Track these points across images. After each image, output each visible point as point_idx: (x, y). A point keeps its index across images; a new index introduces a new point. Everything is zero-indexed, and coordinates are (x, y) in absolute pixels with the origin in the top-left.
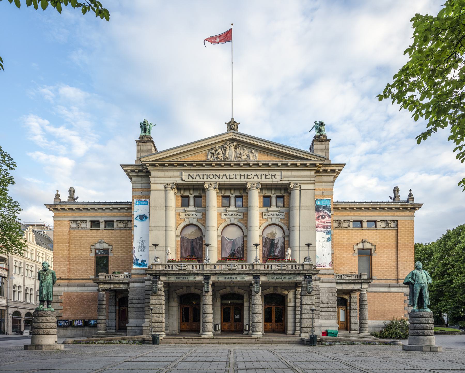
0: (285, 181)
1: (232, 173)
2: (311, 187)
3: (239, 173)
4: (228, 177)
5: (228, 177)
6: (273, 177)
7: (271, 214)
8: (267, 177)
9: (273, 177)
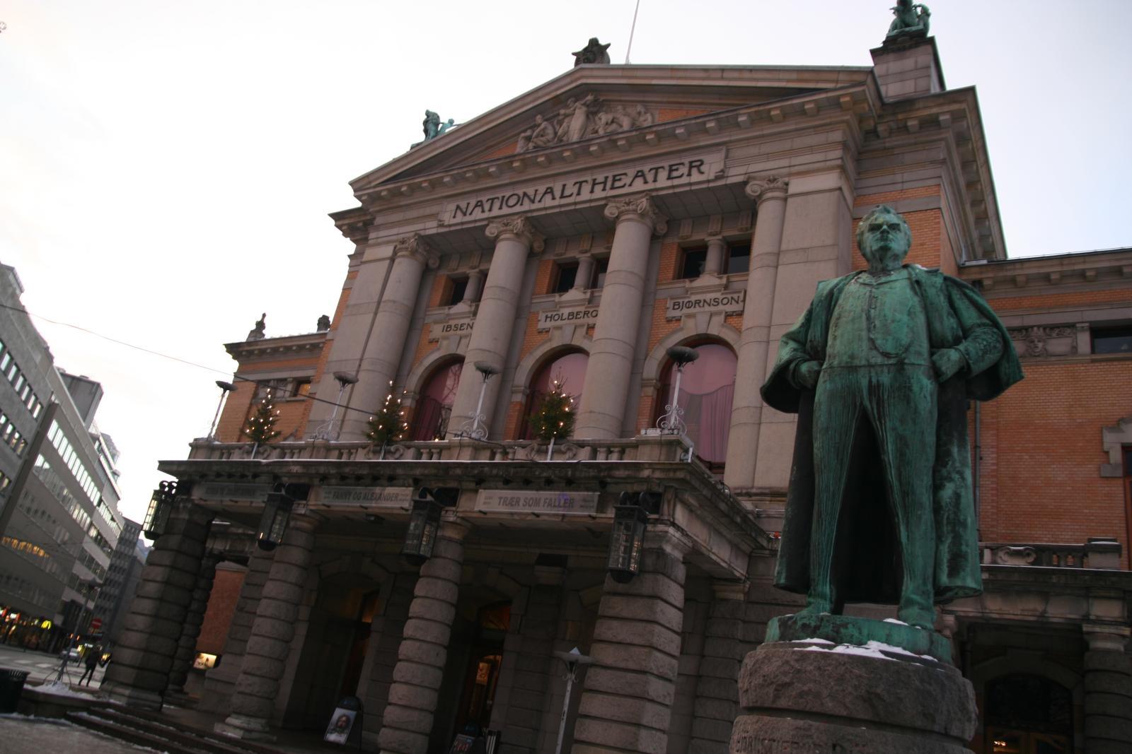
2: (831, 180)
3: (589, 178)
4: (557, 194)
5: (557, 194)
6: (694, 171)
7: (698, 302)
8: (675, 174)
9: (694, 171)
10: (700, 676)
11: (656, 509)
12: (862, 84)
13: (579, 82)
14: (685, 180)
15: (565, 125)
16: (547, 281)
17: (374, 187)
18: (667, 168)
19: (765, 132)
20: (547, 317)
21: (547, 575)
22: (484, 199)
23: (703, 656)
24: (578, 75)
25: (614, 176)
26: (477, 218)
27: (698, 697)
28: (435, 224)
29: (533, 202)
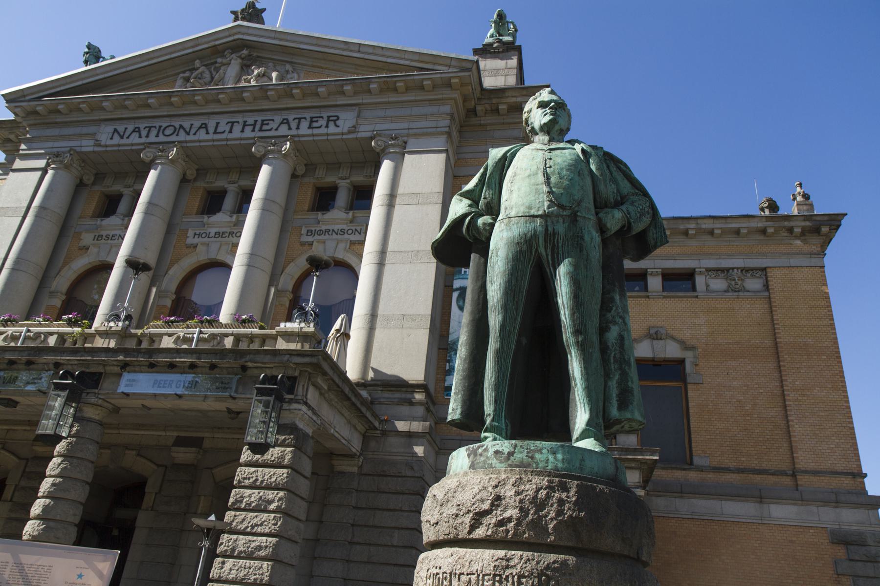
0: (365, 131)
1: (223, 121)
4: (211, 130)
5: (211, 130)
6: (331, 124)
8: (315, 124)
9: (331, 124)
10: (318, 540)
11: (291, 391)
12: (469, 70)
13: (236, 37)
14: (323, 130)
15: (221, 71)
16: (197, 204)
17: (29, 101)
18: (309, 119)
19: (391, 100)
20: (195, 234)
21: (183, 455)
22: (142, 126)
23: (322, 522)
24: (234, 31)
25: (263, 121)
26: (134, 142)
27: (315, 558)
28: (92, 142)
29: (188, 134)
